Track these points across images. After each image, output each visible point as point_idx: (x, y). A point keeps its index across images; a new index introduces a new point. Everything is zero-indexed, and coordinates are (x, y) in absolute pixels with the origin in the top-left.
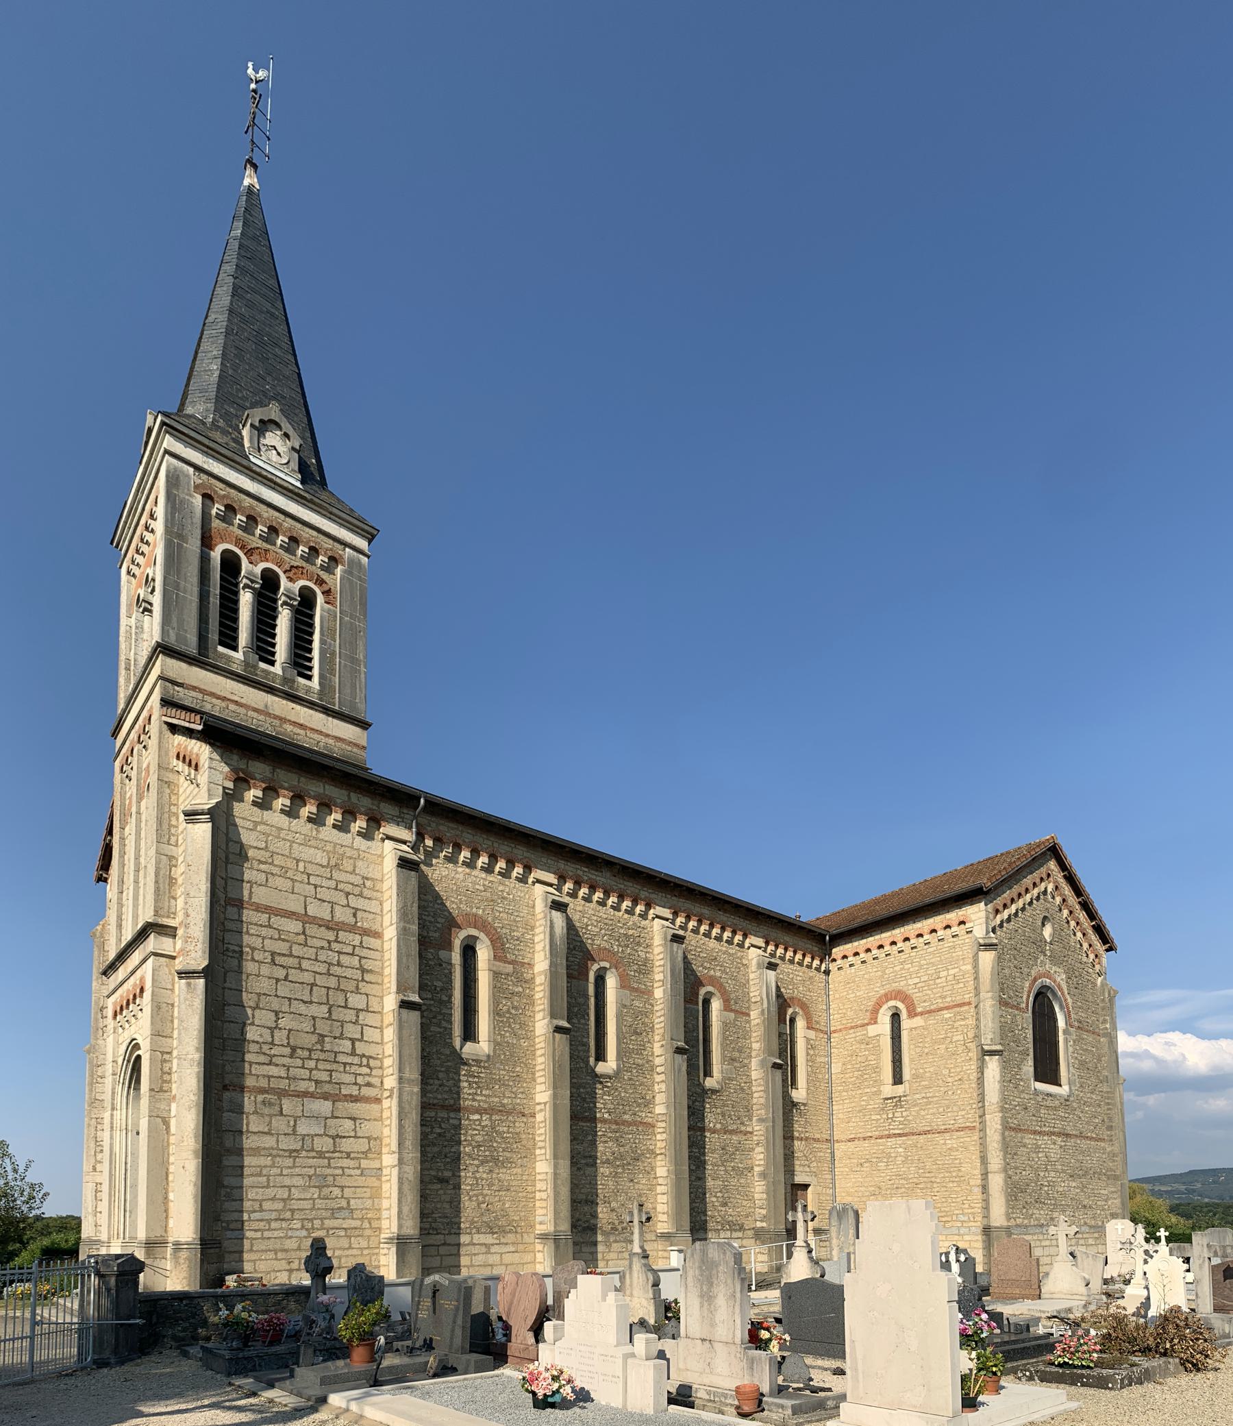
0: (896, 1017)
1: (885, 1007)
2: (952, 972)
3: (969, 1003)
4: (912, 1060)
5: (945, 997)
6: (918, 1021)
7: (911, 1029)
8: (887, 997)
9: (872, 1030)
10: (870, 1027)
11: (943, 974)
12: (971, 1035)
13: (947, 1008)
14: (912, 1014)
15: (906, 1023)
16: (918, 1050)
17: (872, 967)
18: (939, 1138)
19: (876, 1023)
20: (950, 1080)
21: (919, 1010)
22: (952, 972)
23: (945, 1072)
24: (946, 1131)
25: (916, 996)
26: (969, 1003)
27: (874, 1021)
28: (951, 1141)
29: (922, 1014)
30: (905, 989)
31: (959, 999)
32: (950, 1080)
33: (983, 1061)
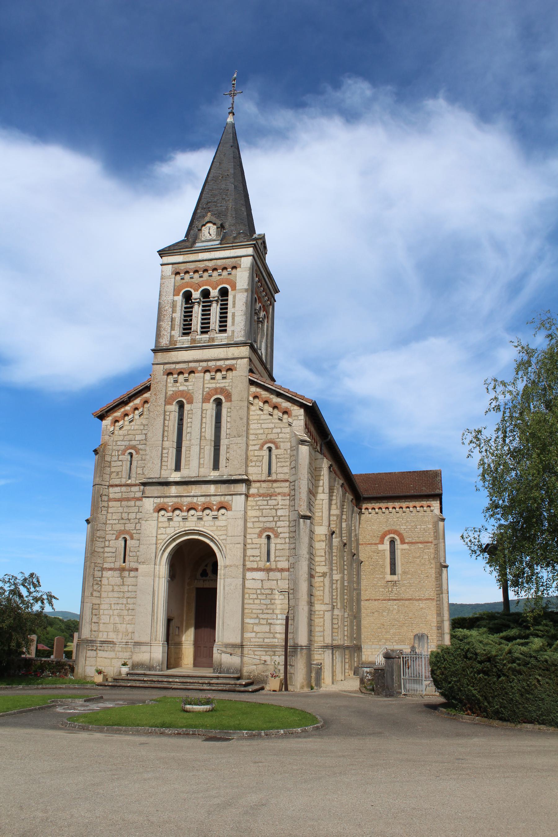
0: (392, 542)
1: (388, 537)
2: (423, 527)
3: (431, 542)
4: (402, 564)
5: (420, 537)
6: (406, 546)
7: (402, 549)
8: (390, 532)
9: (381, 547)
10: (379, 545)
11: (419, 527)
12: (432, 556)
13: (421, 543)
14: (403, 542)
15: (399, 546)
16: (406, 560)
17: (381, 517)
18: (416, 603)
19: (383, 544)
20: (422, 576)
21: (407, 541)
22: (423, 527)
23: (420, 572)
24: (420, 600)
25: (405, 535)
26: (431, 542)
27: (382, 542)
28: (422, 604)
29: (408, 543)
30: (399, 530)
31: (426, 540)
32: (422, 576)
33: (442, 570)
